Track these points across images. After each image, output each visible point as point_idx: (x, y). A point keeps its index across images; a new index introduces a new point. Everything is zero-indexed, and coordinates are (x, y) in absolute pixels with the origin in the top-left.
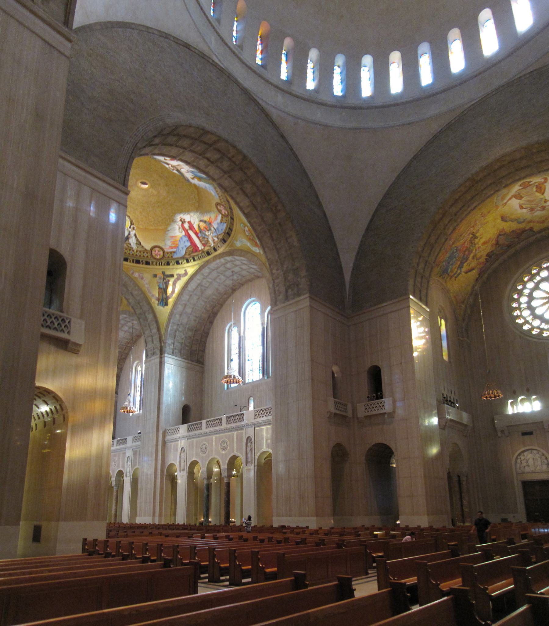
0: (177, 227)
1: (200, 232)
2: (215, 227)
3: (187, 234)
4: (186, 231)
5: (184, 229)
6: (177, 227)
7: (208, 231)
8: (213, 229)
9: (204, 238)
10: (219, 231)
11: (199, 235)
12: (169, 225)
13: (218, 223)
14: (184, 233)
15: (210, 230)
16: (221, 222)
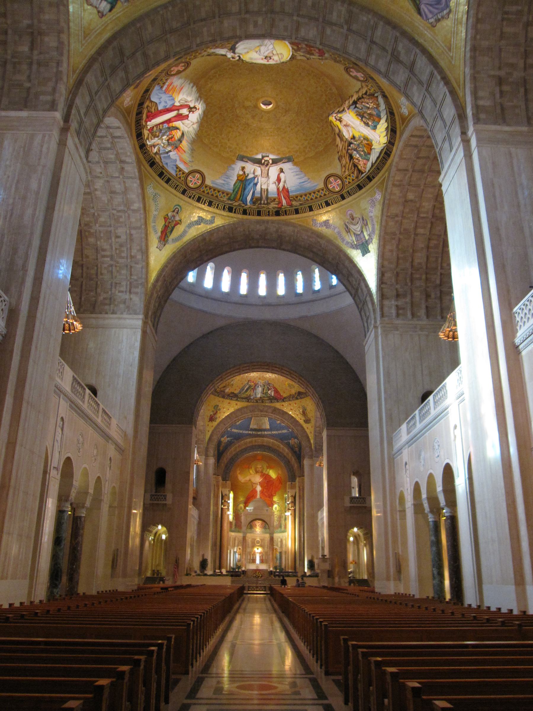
0: (189, 99)
1: (169, 128)
2: (171, 154)
3: (174, 108)
4: (178, 109)
5: (182, 107)
6: (189, 99)
7: (168, 140)
8: (169, 148)
9: (161, 130)
10: (164, 157)
11: (166, 125)
12: (199, 90)
13: (176, 160)
14: (177, 104)
15: (169, 144)
16: (177, 167)
